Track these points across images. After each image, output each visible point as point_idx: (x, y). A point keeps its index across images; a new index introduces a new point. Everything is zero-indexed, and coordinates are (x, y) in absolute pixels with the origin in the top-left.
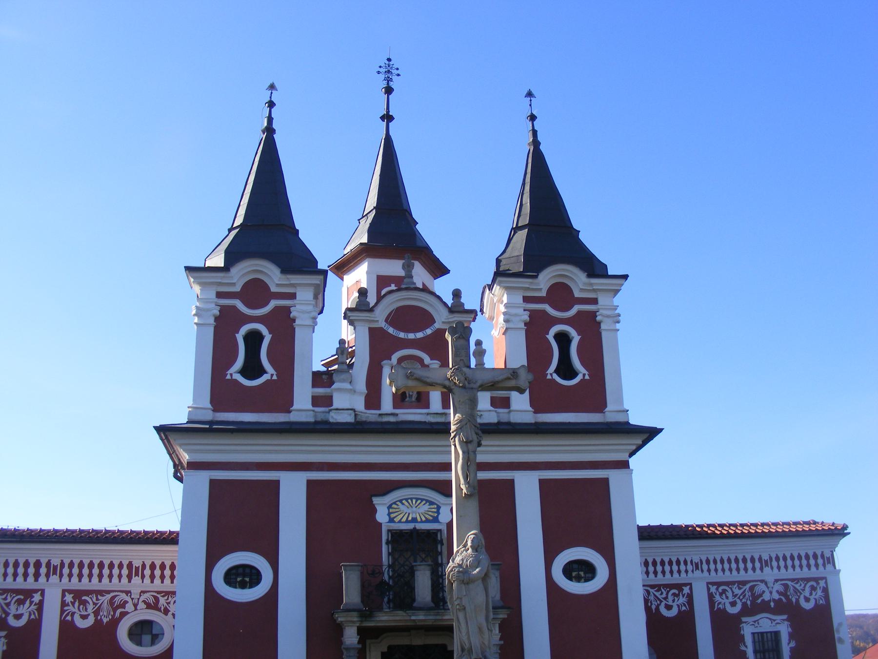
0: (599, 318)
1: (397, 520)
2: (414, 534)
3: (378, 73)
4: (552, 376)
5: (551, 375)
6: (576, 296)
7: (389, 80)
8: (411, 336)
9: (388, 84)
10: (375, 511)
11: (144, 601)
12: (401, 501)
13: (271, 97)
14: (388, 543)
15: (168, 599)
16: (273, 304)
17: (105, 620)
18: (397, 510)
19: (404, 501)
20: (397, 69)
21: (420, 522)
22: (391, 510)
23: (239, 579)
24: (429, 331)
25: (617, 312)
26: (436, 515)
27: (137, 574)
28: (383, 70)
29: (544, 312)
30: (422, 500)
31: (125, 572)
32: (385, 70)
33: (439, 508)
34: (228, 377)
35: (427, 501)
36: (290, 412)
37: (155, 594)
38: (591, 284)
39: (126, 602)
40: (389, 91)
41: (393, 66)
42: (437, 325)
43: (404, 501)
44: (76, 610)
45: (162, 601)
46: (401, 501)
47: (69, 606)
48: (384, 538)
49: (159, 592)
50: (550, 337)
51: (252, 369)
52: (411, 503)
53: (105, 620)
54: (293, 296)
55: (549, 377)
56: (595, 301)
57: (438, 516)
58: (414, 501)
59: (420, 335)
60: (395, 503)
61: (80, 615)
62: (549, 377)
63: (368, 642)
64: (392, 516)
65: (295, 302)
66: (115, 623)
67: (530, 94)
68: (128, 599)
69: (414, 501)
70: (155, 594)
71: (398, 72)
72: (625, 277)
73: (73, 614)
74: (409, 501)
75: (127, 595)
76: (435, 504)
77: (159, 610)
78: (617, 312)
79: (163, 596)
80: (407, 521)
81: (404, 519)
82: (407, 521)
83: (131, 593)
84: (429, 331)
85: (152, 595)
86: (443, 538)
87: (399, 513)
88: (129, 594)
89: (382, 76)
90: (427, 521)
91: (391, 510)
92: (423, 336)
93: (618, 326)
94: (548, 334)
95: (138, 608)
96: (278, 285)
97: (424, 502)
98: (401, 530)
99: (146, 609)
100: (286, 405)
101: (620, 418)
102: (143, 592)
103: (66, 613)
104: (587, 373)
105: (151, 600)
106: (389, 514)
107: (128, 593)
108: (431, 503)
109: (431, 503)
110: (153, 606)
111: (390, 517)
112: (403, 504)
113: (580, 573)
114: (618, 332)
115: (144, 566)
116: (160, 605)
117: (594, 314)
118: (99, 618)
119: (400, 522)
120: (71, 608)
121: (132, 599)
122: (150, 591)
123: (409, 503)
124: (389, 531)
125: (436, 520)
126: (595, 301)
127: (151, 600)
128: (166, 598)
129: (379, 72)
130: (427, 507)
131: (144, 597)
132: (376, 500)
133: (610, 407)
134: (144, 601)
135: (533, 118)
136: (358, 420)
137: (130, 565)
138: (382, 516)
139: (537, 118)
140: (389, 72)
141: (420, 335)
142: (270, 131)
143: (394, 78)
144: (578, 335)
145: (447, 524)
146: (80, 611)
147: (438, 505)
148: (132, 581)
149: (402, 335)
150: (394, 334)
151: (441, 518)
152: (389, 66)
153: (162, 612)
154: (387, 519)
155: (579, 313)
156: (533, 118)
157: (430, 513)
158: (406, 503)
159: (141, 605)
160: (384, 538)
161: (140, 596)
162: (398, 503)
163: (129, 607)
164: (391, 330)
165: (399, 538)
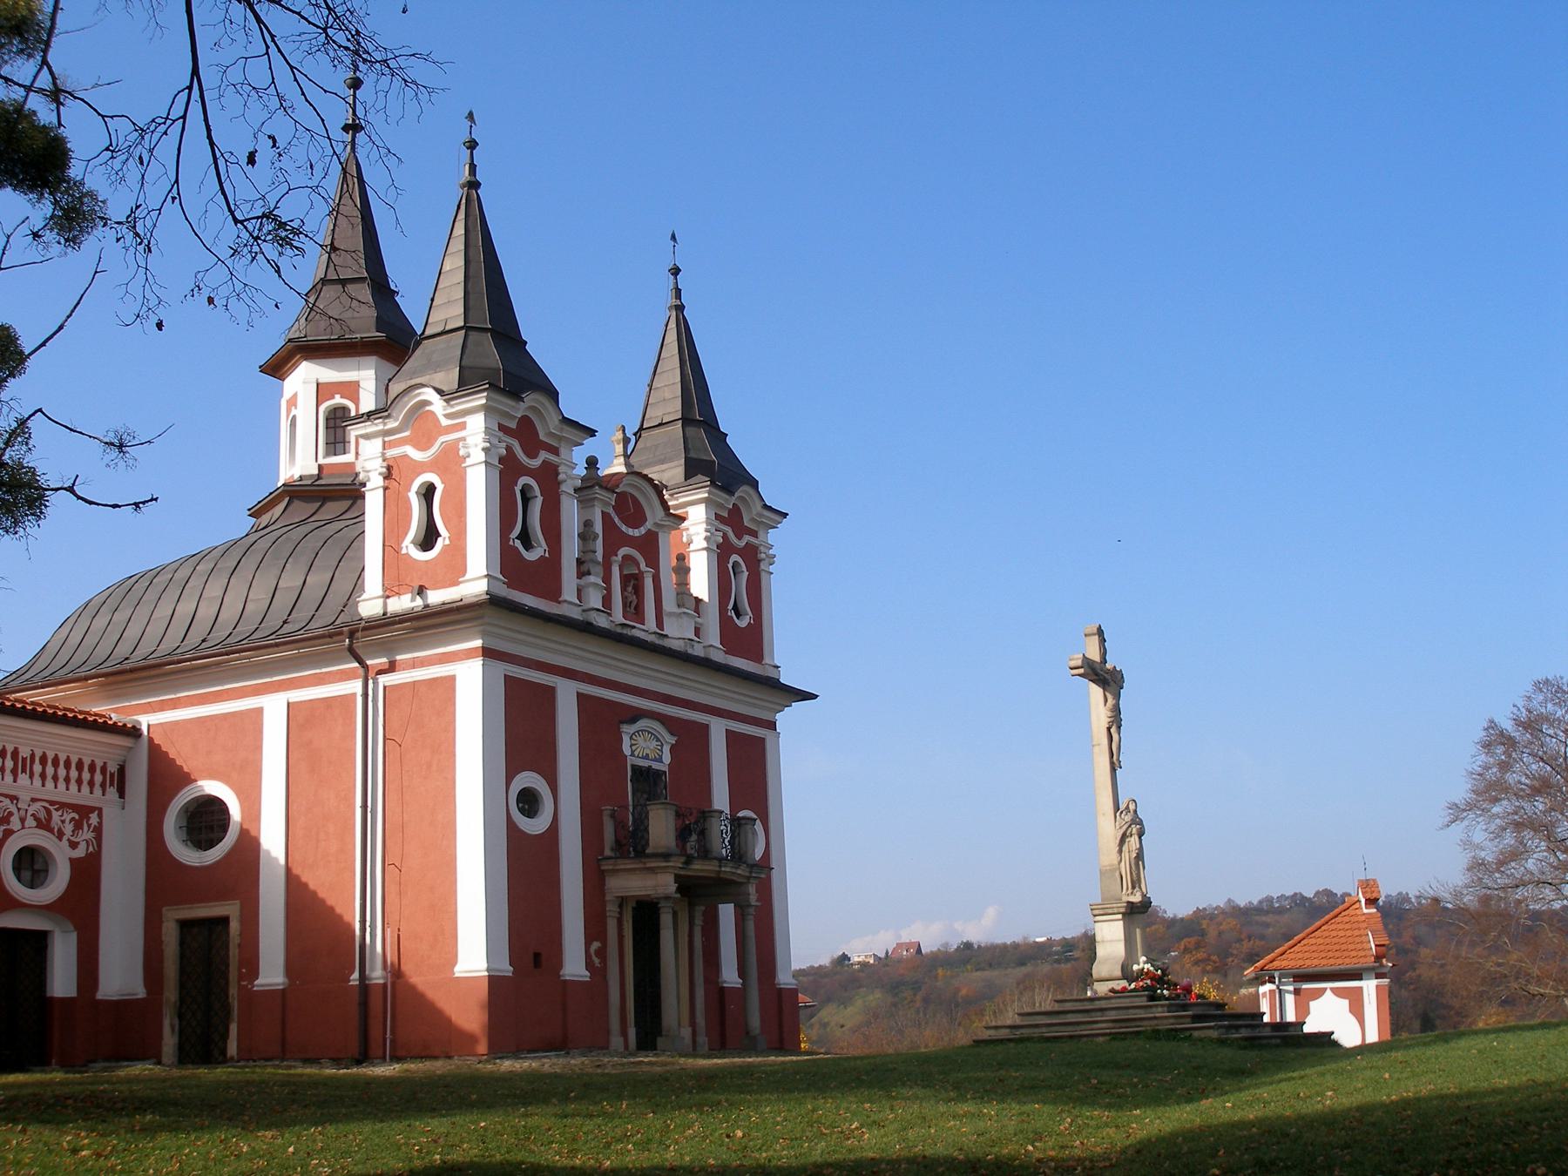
1: (636, 753)
8: (630, 532)
9: (354, 73)
11: (33, 815)
12: (638, 732)
15: (62, 816)
16: (544, 455)
22: (633, 742)
23: (527, 807)
25: (771, 552)
27: (24, 771)
30: (652, 734)
33: (662, 745)
34: (511, 543)
36: (559, 603)
37: (47, 805)
38: (761, 515)
39: (11, 814)
45: (56, 815)
49: (52, 803)
50: (730, 566)
51: (525, 538)
54: (555, 451)
56: (754, 534)
59: (636, 533)
68: (14, 810)
70: (47, 805)
72: (785, 515)
75: (12, 803)
77: (51, 831)
78: (771, 552)
79: (57, 810)
81: (640, 755)
82: (642, 758)
83: (17, 800)
84: (643, 530)
85: (44, 807)
88: (15, 802)
90: (655, 760)
93: (771, 568)
95: (27, 825)
96: (551, 435)
99: (36, 827)
100: (554, 594)
101: (771, 673)
102: (34, 800)
105: (42, 815)
107: (13, 798)
108: (658, 740)
109: (658, 740)
110: (44, 824)
114: (772, 576)
115: (33, 756)
121: (19, 809)
125: (660, 760)
127: (42, 815)
128: (60, 813)
131: (38, 805)
133: (767, 660)
134: (33, 815)
135: (676, 271)
137: (15, 753)
138: (626, 750)
141: (636, 533)
142: (473, 185)
149: (624, 528)
153: (54, 834)
156: (676, 271)
159: (30, 822)
161: (29, 806)
163: (15, 823)
164: (616, 520)
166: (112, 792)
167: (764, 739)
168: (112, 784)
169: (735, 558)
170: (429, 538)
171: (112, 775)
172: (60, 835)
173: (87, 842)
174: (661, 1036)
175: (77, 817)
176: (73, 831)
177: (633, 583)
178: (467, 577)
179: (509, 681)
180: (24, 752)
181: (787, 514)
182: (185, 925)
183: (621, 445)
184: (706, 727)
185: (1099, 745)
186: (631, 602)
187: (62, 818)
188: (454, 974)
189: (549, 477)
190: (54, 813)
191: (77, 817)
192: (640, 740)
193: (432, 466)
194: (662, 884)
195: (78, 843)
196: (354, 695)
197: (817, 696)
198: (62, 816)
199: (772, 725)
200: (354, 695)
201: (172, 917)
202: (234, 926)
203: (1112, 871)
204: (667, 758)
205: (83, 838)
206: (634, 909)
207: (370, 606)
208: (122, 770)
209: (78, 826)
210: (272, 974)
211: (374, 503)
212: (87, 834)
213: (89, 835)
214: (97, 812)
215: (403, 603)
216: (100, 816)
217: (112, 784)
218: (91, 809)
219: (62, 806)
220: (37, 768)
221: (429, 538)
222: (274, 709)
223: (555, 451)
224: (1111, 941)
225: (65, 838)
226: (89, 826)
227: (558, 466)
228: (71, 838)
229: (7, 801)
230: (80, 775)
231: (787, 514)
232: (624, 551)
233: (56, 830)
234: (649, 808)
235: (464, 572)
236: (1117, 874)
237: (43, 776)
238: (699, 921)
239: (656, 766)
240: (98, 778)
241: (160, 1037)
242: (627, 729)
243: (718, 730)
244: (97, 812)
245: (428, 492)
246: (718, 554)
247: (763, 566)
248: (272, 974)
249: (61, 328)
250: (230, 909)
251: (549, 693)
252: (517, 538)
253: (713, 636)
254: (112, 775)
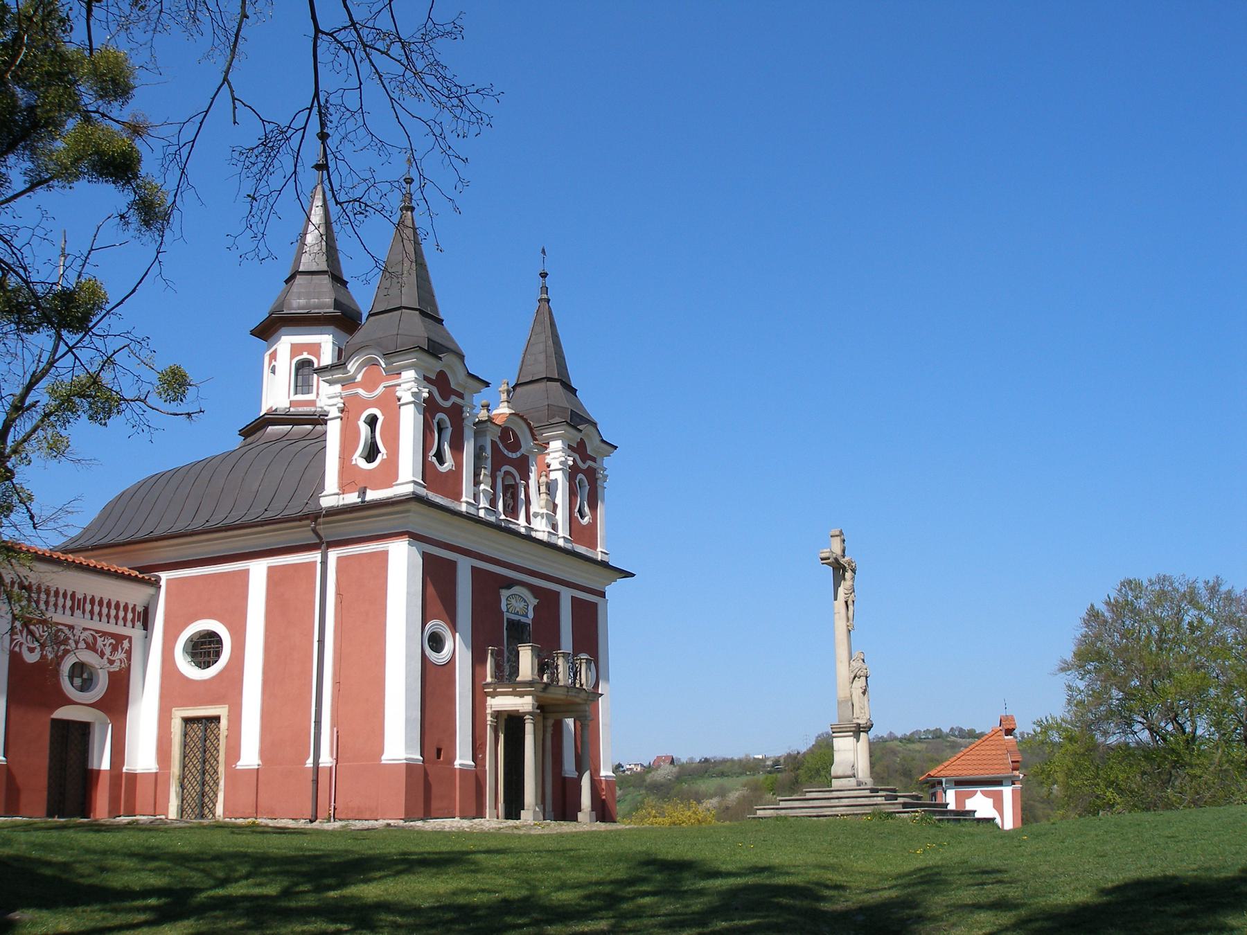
8: (510, 455)
12: (512, 595)
15: (104, 641)
17: (50, 656)
20: (331, 115)
22: (508, 602)
27: (79, 608)
30: (522, 597)
31: (69, 603)
33: (528, 606)
37: (94, 633)
44: (24, 641)
45: (100, 640)
47: (17, 634)
49: (97, 632)
50: (577, 481)
53: (50, 656)
56: (594, 460)
59: (514, 456)
61: (28, 647)
66: (59, 659)
70: (94, 633)
72: (616, 448)
73: (21, 644)
75: (70, 630)
77: (96, 651)
79: (100, 637)
82: (515, 614)
83: (73, 628)
84: (519, 454)
96: (458, 384)
100: (457, 496)
102: (84, 629)
103: (15, 642)
105: (90, 640)
107: (71, 628)
108: (525, 602)
110: (91, 647)
114: (606, 490)
115: (85, 598)
116: (97, 646)
118: (45, 652)
120: (18, 637)
122: (90, 629)
127: (90, 640)
130: (523, 604)
131: (87, 633)
134: (84, 640)
135: (544, 275)
138: (504, 608)
141: (514, 456)
146: (27, 642)
148: (75, 615)
149: (506, 452)
156: (544, 275)
159: (82, 645)
164: (501, 446)
166: (139, 624)
167: (597, 604)
168: (139, 620)
169: (580, 476)
170: (371, 453)
171: (139, 613)
172: (102, 655)
173: (121, 661)
174: (524, 809)
175: (114, 643)
176: (111, 652)
177: (511, 492)
178: (398, 482)
179: (426, 557)
180: (79, 596)
181: (617, 447)
182: (187, 721)
183: (506, 394)
184: (558, 594)
185: (839, 613)
186: (509, 504)
187: (104, 643)
188: (381, 761)
189: (456, 414)
190: (98, 638)
191: (114, 643)
192: (513, 601)
193: (376, 403)
194: (524, 704)
195: (115, 661)
196: (315, 562)
197: (635, 575)
198: (104, 641)
199: (603, 595)
200: (315, 562)
201: (178, 714)
202: (224, 723)
203: (846, 701)
204: (531, 614)
205: (117, 658)
206: (506, 720)
207: (326, 502)
208: (146, 610)
209: (115, 649)
210: (250, 757)
211: (333, 430)
212: (119, 655)
213: (123, 656)
214: (127, 640)
215: (352, 498)
216: (130, 642)
217: (139, 620)
218: (124, 637)
219: (105, 634)
220: (88, 607)
221: (371, 453)
222: (258, 570)
223: (461, 396)
224: (845, 750)
225: (105, 657)
226: (122, 650)
227: (463, 407)
228: (110, 657)
229: (66, 630)
230: (117, 613)
231: (617, 447)
232: (506, 468)
233: (99, 651)
234: (519, 648)
235: (396, 478)
236: (850, 703)
237: (92, 612)
238: (550, 731)
239: (523, 619)
240: (130, 616)
241: (168, 801)
242: (504, 593)
243: (566, 595)
244: (127, 640)
245: (372, 421)
246: (570, 472)
247: (599, 482)
248: (250, 757)
249: (134, 291)
250: (221, 711)
251: (453, 565)
253: (563, 531)
254: (139, 613)
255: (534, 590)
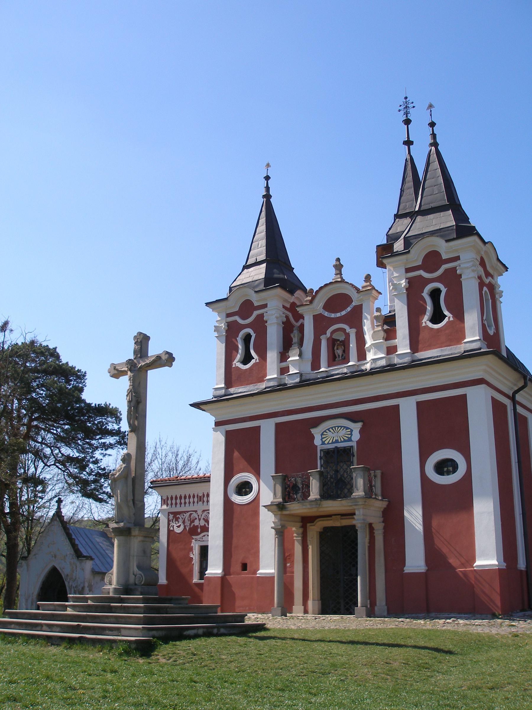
0: (458, 272)
1: (326, 442)
2: (337, 450)
3: (400, 111)
4: (426, 324)
5: (425, 322)
6: (421, 264)
7: (407, 114)
8: (338, 315)
9: (407, 117)
10: (313, 437)
12: (328, 430)
13: (267, 173)
14: (321, 458)
18: (326, 436)
19: (330, 429)
21: (340, 442)
22: (323, 436)
24: (349, 309)
26: (350, 436)
28: (402, 107)
29: (420, 276)
30: (341, 427)
32: (403, 107)
33: (352, 431)
34: (234, 366)
35: (345, 427)
40: (407, 122)
41: (409, 102)
42: (354, 304)
43: (330, 429)
46: (328, 430)
48: (319, 455)
50: (425, 294)
52: (335, 430)
55: (424, 325)
56: (457, 258)
57: (351, 437)
58: (337, 428)
59: (344, 313)
60: (325, 431)
62: (424, 325)
63: (308, 525)
64: (324, 440)
65: (266, 309)
67: (431, 106)
69: (337, 428)
71: (412, 105)
74: (334, 428)
76: (349, 429)
80: (333, 443)
81: (330, 442)
82: (333, 443)
84: (349, 309)
86: (354, 451)
87: (328, 437)
89: (402, 112)
90: (345, 441)
91: (323, 436)
92: (345, 313)
94: (423, 293)
96: (257, 301)
97: (343, 428)
98: (328, 449)
104: (451, 316)
106: (322, 438)
108: (347, 428)
111: (322, 441)
112: (330, 431)
113: (449, 468)
117: (454, 269)
119: (328, 443)
123: (333, 430)
124: (321, 450)
125: (350, 440)
126: (457, 258)
129: (400, 111)
132: (313, 431)
135: (432, 125)
136: (303, 379)
138: (317, 441)
139: (436, 124)
140: (406, 107)
141: (344, 313)
142: (267, 197)
143: (411, 110)
144: (445, 288)
145: (357, 441)
147: (351, 429)
149: (333, 315)
150: (328, 316)
151: (353, 439)
152: (406, 103)
154: (320, 442)
155: (446, 271)
156: (432, 125)
157: (346, 435)
158: (332, 431)
160: (319, 455)
162: (327, 431)
164: (326, 314)
165: (328, 454)
184: (397, 407)
204: (356, 436)
242: (316, 432)
252: (237, 362)
255: (352, 417)
